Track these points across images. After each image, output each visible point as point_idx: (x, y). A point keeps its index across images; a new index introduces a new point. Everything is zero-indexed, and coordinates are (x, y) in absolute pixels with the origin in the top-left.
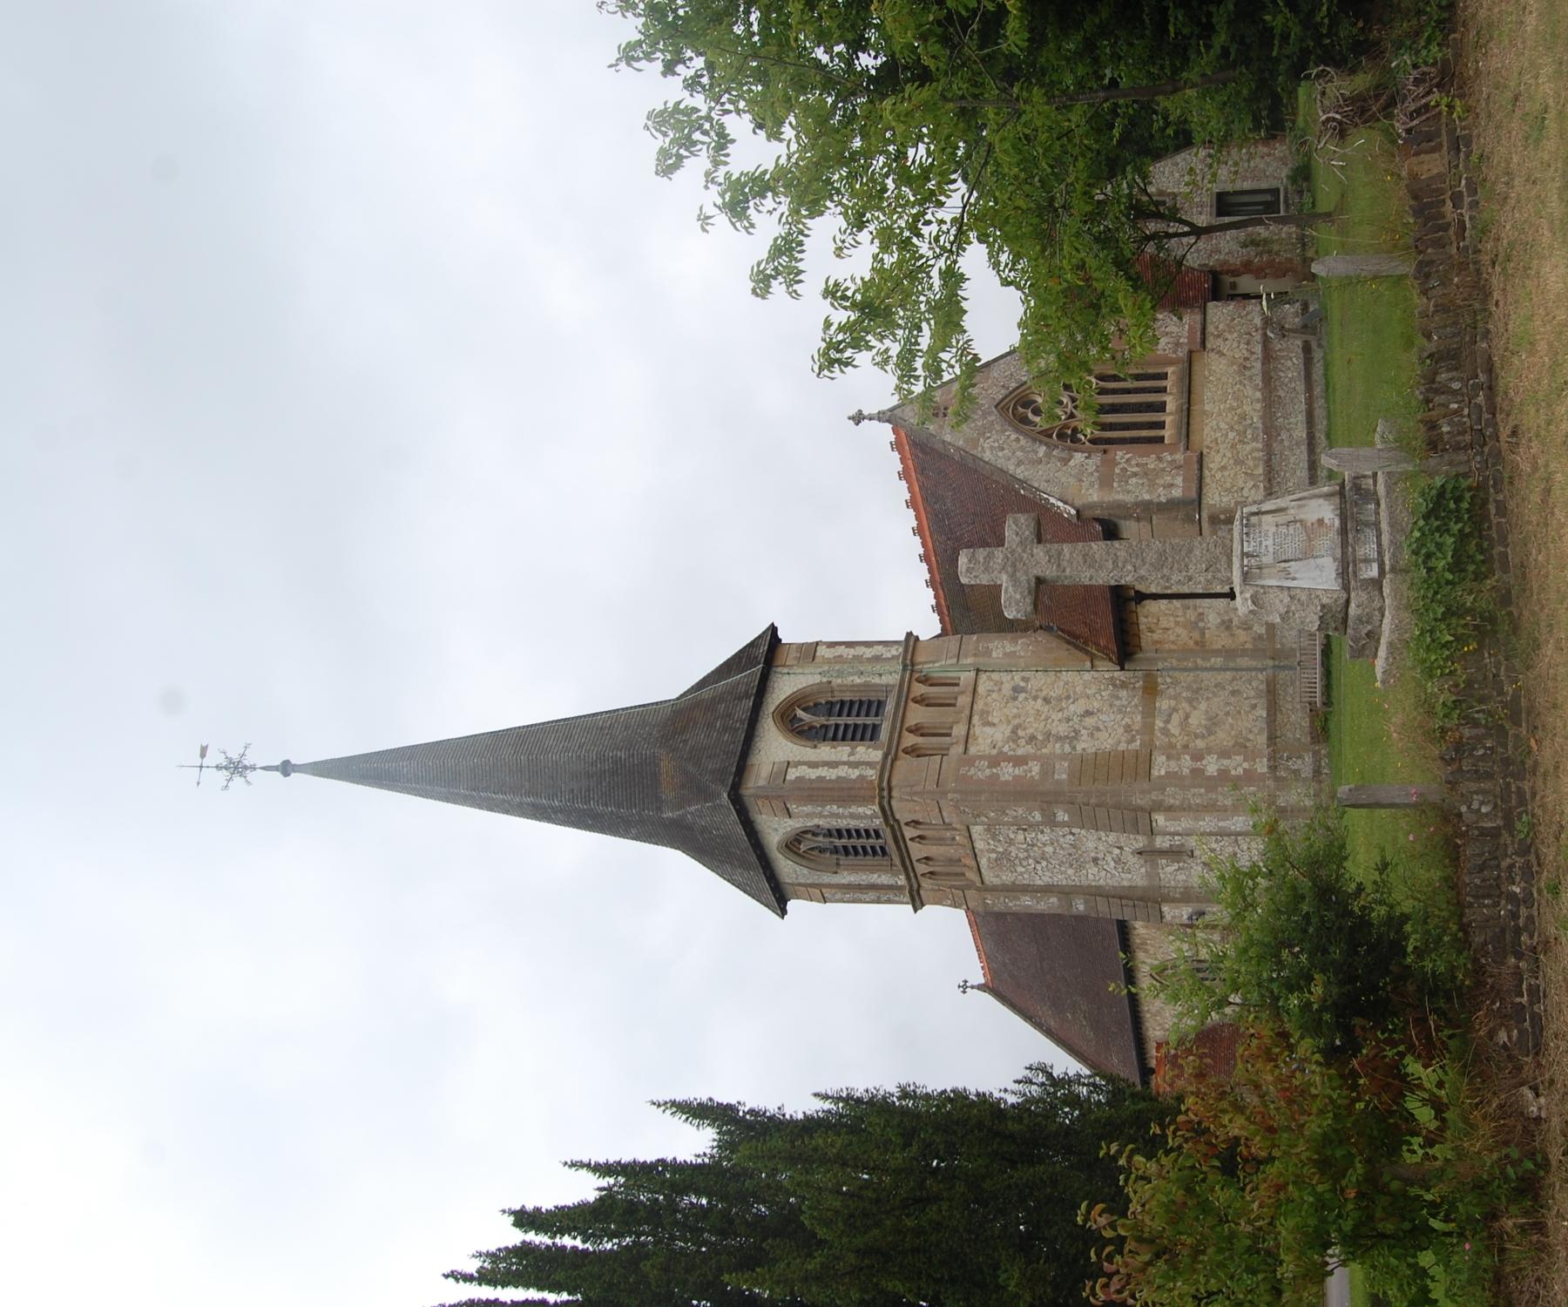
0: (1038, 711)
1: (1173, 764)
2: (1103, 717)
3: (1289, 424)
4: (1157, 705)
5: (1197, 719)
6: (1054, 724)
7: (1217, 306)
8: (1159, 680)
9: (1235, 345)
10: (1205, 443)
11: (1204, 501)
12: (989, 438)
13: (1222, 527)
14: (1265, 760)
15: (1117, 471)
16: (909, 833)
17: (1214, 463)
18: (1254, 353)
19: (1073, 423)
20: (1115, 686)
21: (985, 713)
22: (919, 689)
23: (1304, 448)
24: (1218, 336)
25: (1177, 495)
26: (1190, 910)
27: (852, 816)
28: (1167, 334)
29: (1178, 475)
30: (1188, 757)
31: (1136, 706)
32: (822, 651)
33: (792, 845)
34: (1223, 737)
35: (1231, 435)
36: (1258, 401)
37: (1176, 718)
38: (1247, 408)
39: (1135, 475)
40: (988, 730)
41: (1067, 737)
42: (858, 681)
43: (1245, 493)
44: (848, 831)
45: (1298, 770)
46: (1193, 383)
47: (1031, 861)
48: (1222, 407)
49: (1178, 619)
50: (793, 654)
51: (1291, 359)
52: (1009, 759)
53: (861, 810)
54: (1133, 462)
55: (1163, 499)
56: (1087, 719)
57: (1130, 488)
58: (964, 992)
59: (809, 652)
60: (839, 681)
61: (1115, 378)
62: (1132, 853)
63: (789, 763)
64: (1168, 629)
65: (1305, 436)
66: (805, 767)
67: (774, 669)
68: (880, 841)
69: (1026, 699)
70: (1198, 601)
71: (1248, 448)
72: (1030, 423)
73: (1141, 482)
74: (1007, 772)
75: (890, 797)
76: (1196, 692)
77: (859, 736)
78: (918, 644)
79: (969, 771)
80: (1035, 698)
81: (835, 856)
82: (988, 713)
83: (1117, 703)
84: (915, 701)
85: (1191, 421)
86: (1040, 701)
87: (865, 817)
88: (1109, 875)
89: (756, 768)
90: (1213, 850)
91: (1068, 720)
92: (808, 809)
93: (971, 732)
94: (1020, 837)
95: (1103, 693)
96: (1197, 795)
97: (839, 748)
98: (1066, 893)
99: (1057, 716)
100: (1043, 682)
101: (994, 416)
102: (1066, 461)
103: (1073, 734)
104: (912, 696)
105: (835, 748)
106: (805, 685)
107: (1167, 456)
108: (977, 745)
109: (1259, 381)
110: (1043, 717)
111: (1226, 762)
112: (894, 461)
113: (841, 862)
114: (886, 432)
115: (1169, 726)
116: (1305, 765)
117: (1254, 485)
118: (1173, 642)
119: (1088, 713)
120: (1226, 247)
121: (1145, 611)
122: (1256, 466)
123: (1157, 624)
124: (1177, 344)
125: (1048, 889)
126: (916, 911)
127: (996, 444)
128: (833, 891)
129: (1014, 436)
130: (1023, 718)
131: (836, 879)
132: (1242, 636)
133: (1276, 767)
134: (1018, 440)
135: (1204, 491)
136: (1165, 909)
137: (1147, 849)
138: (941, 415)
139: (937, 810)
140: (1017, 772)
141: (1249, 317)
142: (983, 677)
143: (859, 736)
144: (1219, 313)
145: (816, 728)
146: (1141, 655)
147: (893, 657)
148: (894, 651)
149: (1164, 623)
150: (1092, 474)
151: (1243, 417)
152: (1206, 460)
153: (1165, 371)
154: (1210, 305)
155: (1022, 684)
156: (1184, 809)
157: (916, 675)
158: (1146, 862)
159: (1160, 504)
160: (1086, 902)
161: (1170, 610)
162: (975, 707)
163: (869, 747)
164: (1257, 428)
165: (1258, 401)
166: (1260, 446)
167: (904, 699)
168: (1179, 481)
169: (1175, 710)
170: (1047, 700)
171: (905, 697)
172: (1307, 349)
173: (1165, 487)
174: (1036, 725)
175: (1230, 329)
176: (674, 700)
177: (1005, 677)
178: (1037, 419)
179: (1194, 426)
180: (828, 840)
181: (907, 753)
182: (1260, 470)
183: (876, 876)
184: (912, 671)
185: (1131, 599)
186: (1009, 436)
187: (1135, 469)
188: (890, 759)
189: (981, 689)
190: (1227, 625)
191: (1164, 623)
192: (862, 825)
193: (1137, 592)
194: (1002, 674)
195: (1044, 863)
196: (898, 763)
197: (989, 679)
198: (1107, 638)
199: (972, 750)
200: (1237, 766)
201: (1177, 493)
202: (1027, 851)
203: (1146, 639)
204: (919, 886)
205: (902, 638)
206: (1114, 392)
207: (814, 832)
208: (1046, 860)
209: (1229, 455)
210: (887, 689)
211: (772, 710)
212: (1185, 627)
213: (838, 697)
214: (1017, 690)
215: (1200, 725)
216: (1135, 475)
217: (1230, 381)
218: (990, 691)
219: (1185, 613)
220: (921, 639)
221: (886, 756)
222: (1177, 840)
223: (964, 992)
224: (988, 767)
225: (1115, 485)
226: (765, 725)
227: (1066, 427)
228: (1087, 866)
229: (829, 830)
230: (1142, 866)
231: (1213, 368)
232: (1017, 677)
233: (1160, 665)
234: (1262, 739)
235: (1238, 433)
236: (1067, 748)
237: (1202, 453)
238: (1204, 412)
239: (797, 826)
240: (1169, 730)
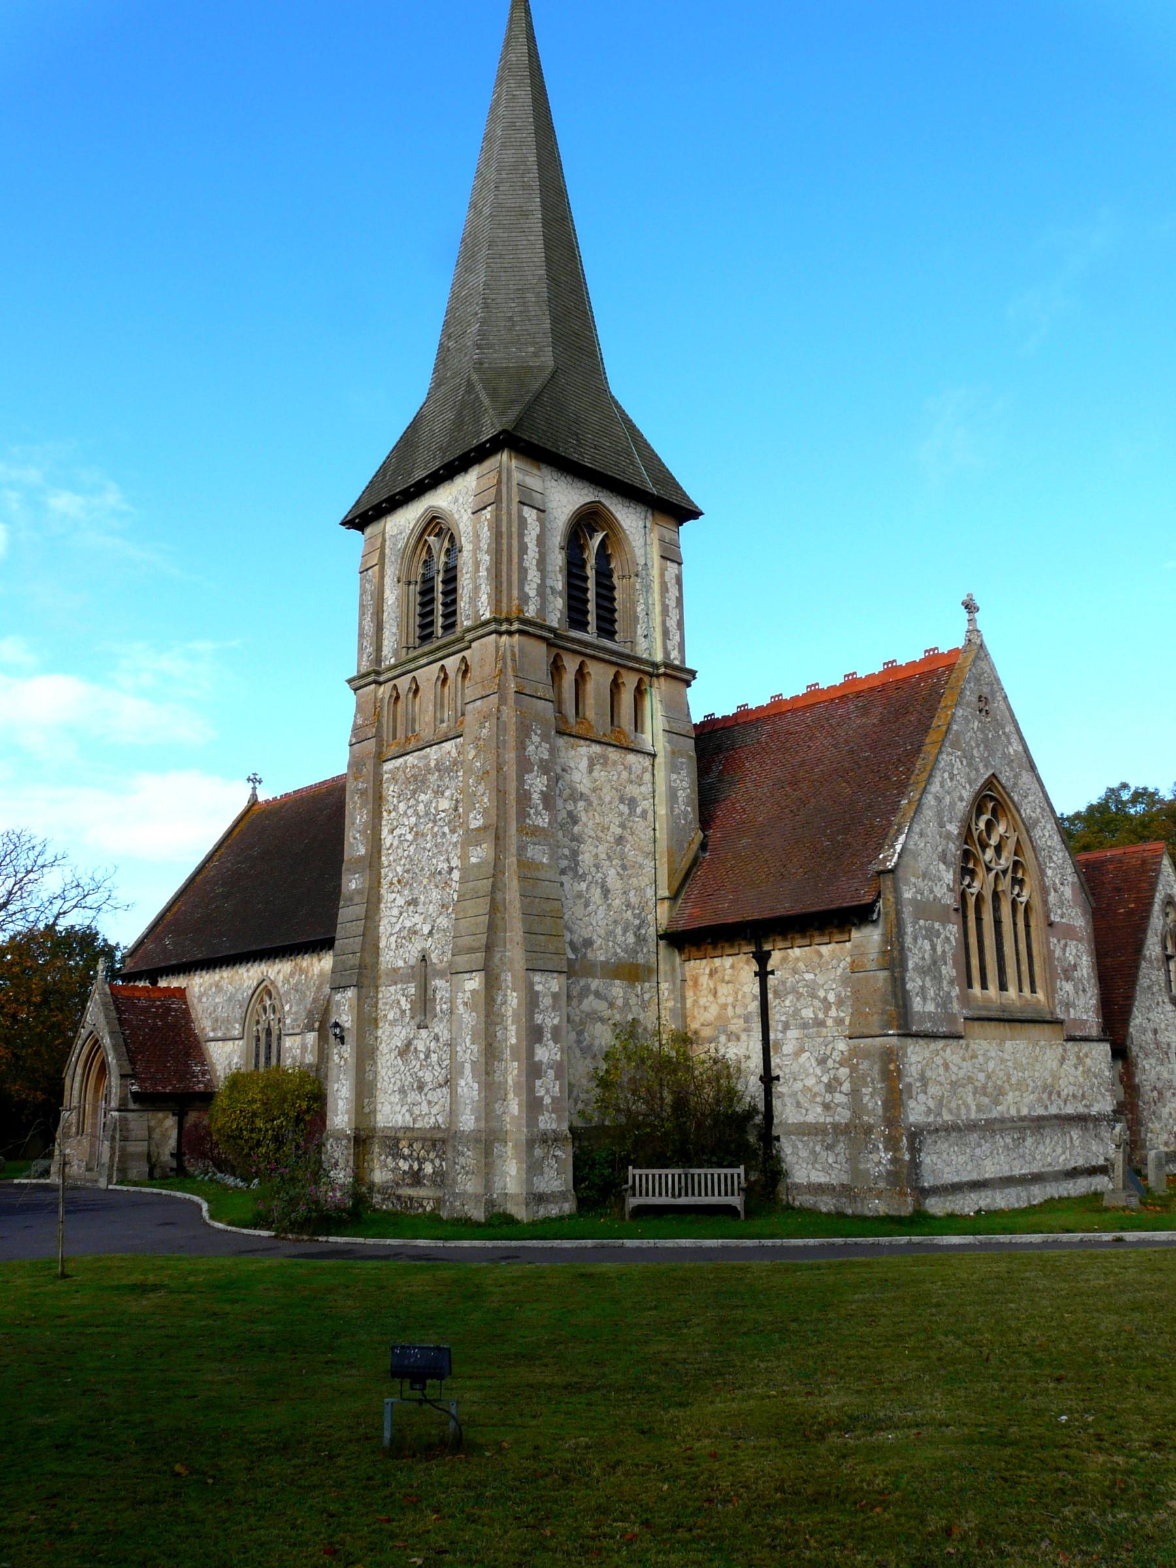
0: (608, 828)
1: (546, 1001)
2: (601, 912)
3: (998, 1154)
4: (617, 982)
6: (591, 848)
7: (1106, 1055)
8: (647, 985)
9: (1072, 1079)
10: (972, 1042)
11: (909, 1041)
12: (962, 762)
13: (876, 1068)
14: (554, 1126)
15: (937, 925)
16: (452, 663)
17: (951, 1052)
18: (1065, 1104)
19: (981, 871)
20: (639, 927)
22: (630, 681)
23: (974, 1176)
24: (1078, 1058)
25: (915, 1005)
26: (347, 1025)
27: (477, 588)
28: (1077, 993)
29: (937, 1005)
30: (556, 1021)
31: (616, 954)
32: (672, 568)
33: (434, 524)
35: (981, 1076)
36: (1018, 1111)
37: (601, 1006)
38: (1010, 1097)
39: (934, 948)
40: (584, 764)
41: (577, 864)
42: (639, 609)
43: (922, 1098)
44: (454, 590)
45: (542, 1174)
46: (1018, 1025)
47: (413, 820)
48: (1009, 1064)
49: (730, 1009)
50: (668, 535)
51: (1064, 1153)
53: (484, 598)
54: (947, 947)
55: (909, 986)
56: (599, 890)
57: (920, 941)
58: (249, 779)
59: (671, 555)
60: (638, 586)
61: (1027, 926)
62: (423, 950)
63: (543, 511)
64: (715, 994)
65: (987, 1176)
66: (538, 529)
67: (650, 511)
68: (440, 631)
69: (621, 814)
70: (757, 1034)
71: (970, 1100)
72: (978, 817)
73: (927, 956)
75: (500, 633)
77: (574, 603)
78: (681, 685)
79: (536, 734)
80: (623, 826)
81: (419, 579)
82: (605, 764)
83: (619, 931)
84: (617, 675)
85: (993, 1024)
86: (619, 831)
87: (474, 600)
88: (394, 920)
89: (536, 472)
90: (427, 1056)
91: (597, 867)
92: (486, 533)
93: (582, 742)
94: (445, 804)
95: (629, 912)
97: (560, 577)
99: (602, 849)
100: (643, 837)
102: (943, 858)
103: (581, 871)
104: (623, 671)
105: (561, 571)
106: (634, 544)
107: (956, 991)
108: (567, 749)
109: (1041, 1111)
110: (601, 834)
111: (551, 1073)
112: (909, 653)
113: (412, 587)
114: (951, 639)
115: (592, 997)
117: (929, 1109)
118: (696, 1002)
119: (606, 892)
121: (741, 965)
122: (950, 1111)
123: (723, 981)
124: (1068, 1005)
126: (349, 681)
127: (956, 772)
128: (376, 580)
129: (965, 794)
130: (598, 808)
131: (389, 581)
133: (545, 1142)
134: (961, 799)
135: (921, 1042)
136: (350, 993)
137: (429, 968)
138: (982, 705)
139: (484, 693)
140: (536, 796)
141: (1099, 1097)
142: (647, 762)
143: (574, 603)
145: (582, 553)
146: (678, 960)
147: (667, 653)
148: (674, 654)
149: (723, 989)
150: (932, 891)
151: (1001, 1092)
152: (953, 1043)
153: (1038, 990)
154: (1107, 1047)
155: (639, 810)
156: (487, 1016)
157: (646, 679)
158: (412, 967)
159: (903, 983)
160: (358, 892)
161: (744, 996)
162: (611, 749)
163: (561, 612)
164: (991, 1111)
165: (1018, 1111)
166: (973, 1116)
167: (620, 661)
168: (931, 1007)
169: (611, 1005)
170: (620, 840)
171: (625, 662)
173: (923, 987)
174: (590, 824)
175: (1086, 1072)
176: (610, 392)
177: (646, 789)
178: (982, 825)
179: (991, 1028)
180: (441, 567)
181: (555, 659)
182: (947, 1117)
183: (394, 630)
184: (651, 675)
185: (759, 946)
186: (964, 787)
187: (939, 950)
189: (631, 758)
191: (723, 989)
192: (463, 604)
193: (768, 954)
194: (650, 785)
195: (410, 837)
196: (544, 647)
197: (645, 770)
201: (917, 1004)
202: (427, 814)
203: (699, 968)
204: (380, 684)
205: (689, 665)
207: (453, 550)
208: (415, 839)
209: (961, 1074)
211: (603, 500)
212: (719, 1017)
215: (593, 1038)
216: (934, 948)
217: (1037, 1074)
218: (629, 769)
219: (740, 1016)
220: (688, 689)
221: (551, 630)
222: (441, 1007)
223: (249, 779)
224: (541, 760)
225: (922, 922)
226: (585, 491)
227: (977, 862)
228: (406, 892)
229: (455, 567)
230: (405, 962)
231: (1048, 1051)
232: (646, 804)
233: (664, 986)
235: (984, 1087)
236: (564, 863)
237: (960, 1037)
238: (1003, 1041)
239: (461, 526)
240: (587, 997)
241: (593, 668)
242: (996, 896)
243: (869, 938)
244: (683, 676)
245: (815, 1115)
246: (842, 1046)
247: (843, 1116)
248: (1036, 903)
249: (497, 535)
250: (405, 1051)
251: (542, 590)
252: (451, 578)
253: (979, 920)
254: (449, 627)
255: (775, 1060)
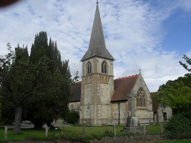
5: (104, 110)
21: (105, 85)
22: (108, 77)
32: (112, 66)
33: (89, 62)
34: (102, 113)
52: (100, 88)
59: (112, 64)
61: (145, 101)
74: (98, 88)
76: (108, 110)
96: (95, 110)
98: (83, 95)
101: (140, 87)
109: (144, 118)
112: (134, 74)
114: (138, 74)
116: (99, 123)
120: (160, 114)
125: (84, 93)
132: (114, 116)
144: (152, 113)
171: (107, 76)
172: (148, 123)
177: (109, 88)
188: (100, 74)
190: (115, 114)
192: (92, 71)
198: (114, 100)
199: (101, 84)
200: (99, 115)
203: (114, 104)
206: (143, 101)
210: (108, 74)
213: (107, 68)
214: (108, 89)
234: (102, 118)
241: (104, 76)
242: (141, 98)
243: (127, 103)
244: (113, 76)
245: (123, 118)
246: (125, 112)
247: (125, 118)
248: (146, 99)
249: (95, 64)
250: (87, 112)
251: (99, 70)
252: (91, 68)
253: (139, 100)
254: (91, 72)
255: (120, 113)
